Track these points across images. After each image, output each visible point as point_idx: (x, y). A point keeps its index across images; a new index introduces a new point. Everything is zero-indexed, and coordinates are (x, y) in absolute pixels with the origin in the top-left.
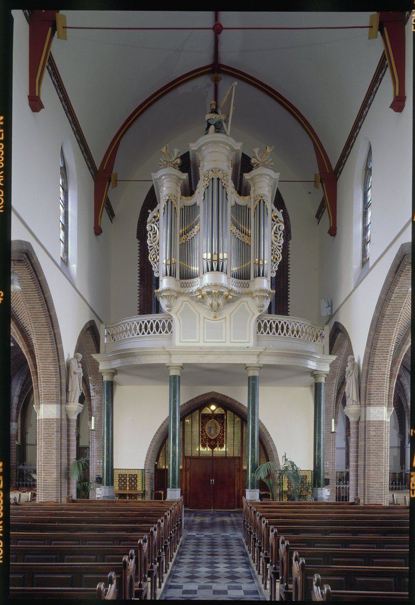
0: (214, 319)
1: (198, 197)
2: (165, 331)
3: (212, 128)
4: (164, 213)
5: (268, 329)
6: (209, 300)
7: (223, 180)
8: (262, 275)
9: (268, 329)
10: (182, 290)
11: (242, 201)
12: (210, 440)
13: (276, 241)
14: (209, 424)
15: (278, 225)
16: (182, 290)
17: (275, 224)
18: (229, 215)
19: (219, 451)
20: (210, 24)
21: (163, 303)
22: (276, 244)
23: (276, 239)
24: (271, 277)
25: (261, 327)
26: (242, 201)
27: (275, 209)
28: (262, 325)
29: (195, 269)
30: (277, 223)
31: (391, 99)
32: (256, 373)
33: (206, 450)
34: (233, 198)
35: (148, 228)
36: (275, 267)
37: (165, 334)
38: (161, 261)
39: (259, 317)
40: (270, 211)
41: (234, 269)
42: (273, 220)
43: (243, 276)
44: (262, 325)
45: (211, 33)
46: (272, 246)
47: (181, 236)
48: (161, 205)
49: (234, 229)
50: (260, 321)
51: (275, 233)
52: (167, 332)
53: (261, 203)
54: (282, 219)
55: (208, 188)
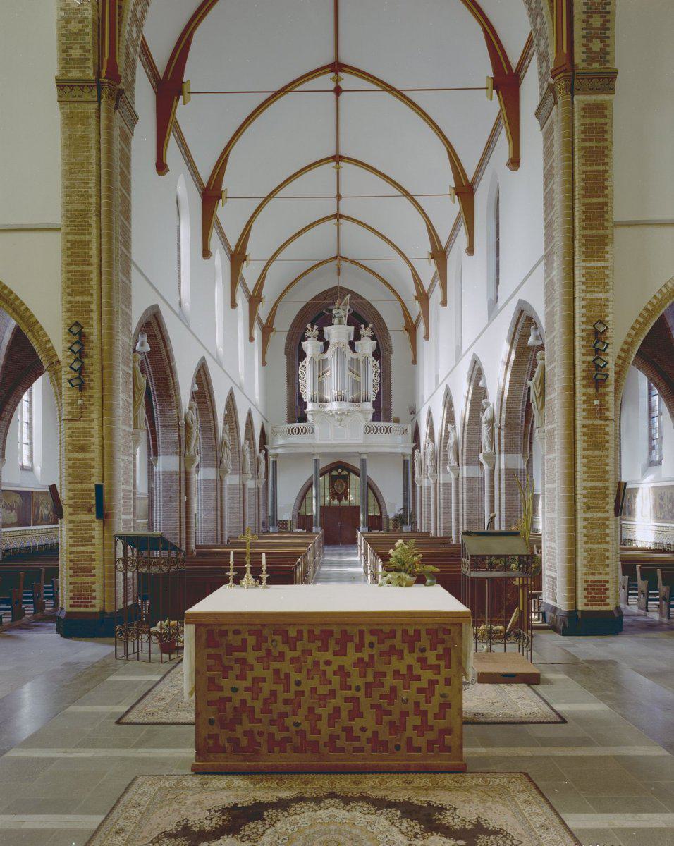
3: (336, 321)
6: (336, 417)
8: (366, 400)
10: (321, 409)
11: (354, 356)
12: (338, 494)
14: (337, 482)
16: (321, 409)
18: (346, 366)
19: (344, 502)
20: (332, 86)
21: (309, 417)
25: (368, 430)
26: (354, 356)
27: (375, 361)
29: (327, 397)
31: (440, 299)
32: (365, 457)
33: (336, 502)
34: (350, 354)
35: (300, 372)
38: (308, 393)
40: (371, 362)
45: (334, 201)
48: (307, 359)
53: (366, 358)
54: (379, 366)
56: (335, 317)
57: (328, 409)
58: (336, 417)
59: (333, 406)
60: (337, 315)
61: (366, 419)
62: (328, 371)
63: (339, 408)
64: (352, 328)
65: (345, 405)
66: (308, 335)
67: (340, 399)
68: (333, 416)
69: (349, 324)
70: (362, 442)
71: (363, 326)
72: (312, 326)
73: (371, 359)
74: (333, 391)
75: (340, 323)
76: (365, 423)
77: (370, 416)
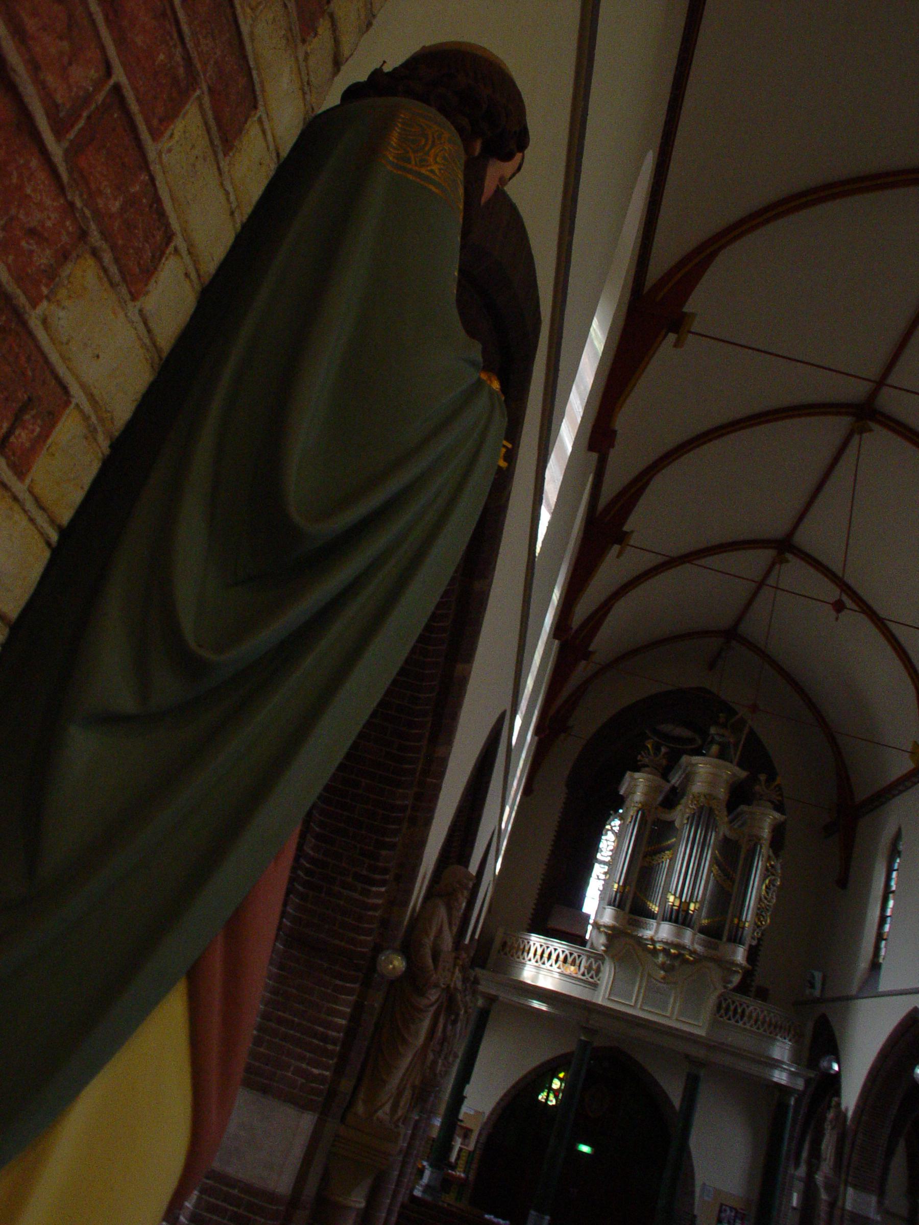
0: (662, 981)
1: (680, 816)
2: (590, 975)
3: (715, 748)
4: (630, 822)
5: (731, 1013)
7: (716, 812)
9: (731, 1013)
13: (766, 898)
15: (773, 877)
17: (769, 876)
22: (766, 902)
23: (766, 895)
24: (750, 946)
28: (724, 1005)
30: (773, 875)
36: (757, 933)
37: (591, 980)
39: (721, 995)
41: (705, 922)
42: (767, 869)
43: (712, 933)
44: (724, 1005)
46: (759, 903)
47: (645, 856)
49: (715, 868)
50: (722, 999)
51: (766, 887)
52: (592, 977)
55: (694, 814)
56: (712, 741)
57: (648, 933)
58: (661, 959)
59: (663, 932)
60: (717, 738)
61: (727, 981)
62: (669, 848)
63: (676, 940)
64: (743, 774)
65: (688, 937)
66: (646, 760)
67: (679, 918)
68: (655, 952)
69: (739, 765)
70: (701, 1032)
71: (763, 777)
72: (657, 748)
73: (765, 849)
74: (671, 898)
75: (722, 755)
76: (721, 990)
77: (736, 979)
